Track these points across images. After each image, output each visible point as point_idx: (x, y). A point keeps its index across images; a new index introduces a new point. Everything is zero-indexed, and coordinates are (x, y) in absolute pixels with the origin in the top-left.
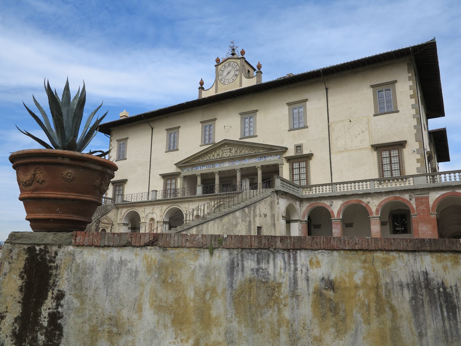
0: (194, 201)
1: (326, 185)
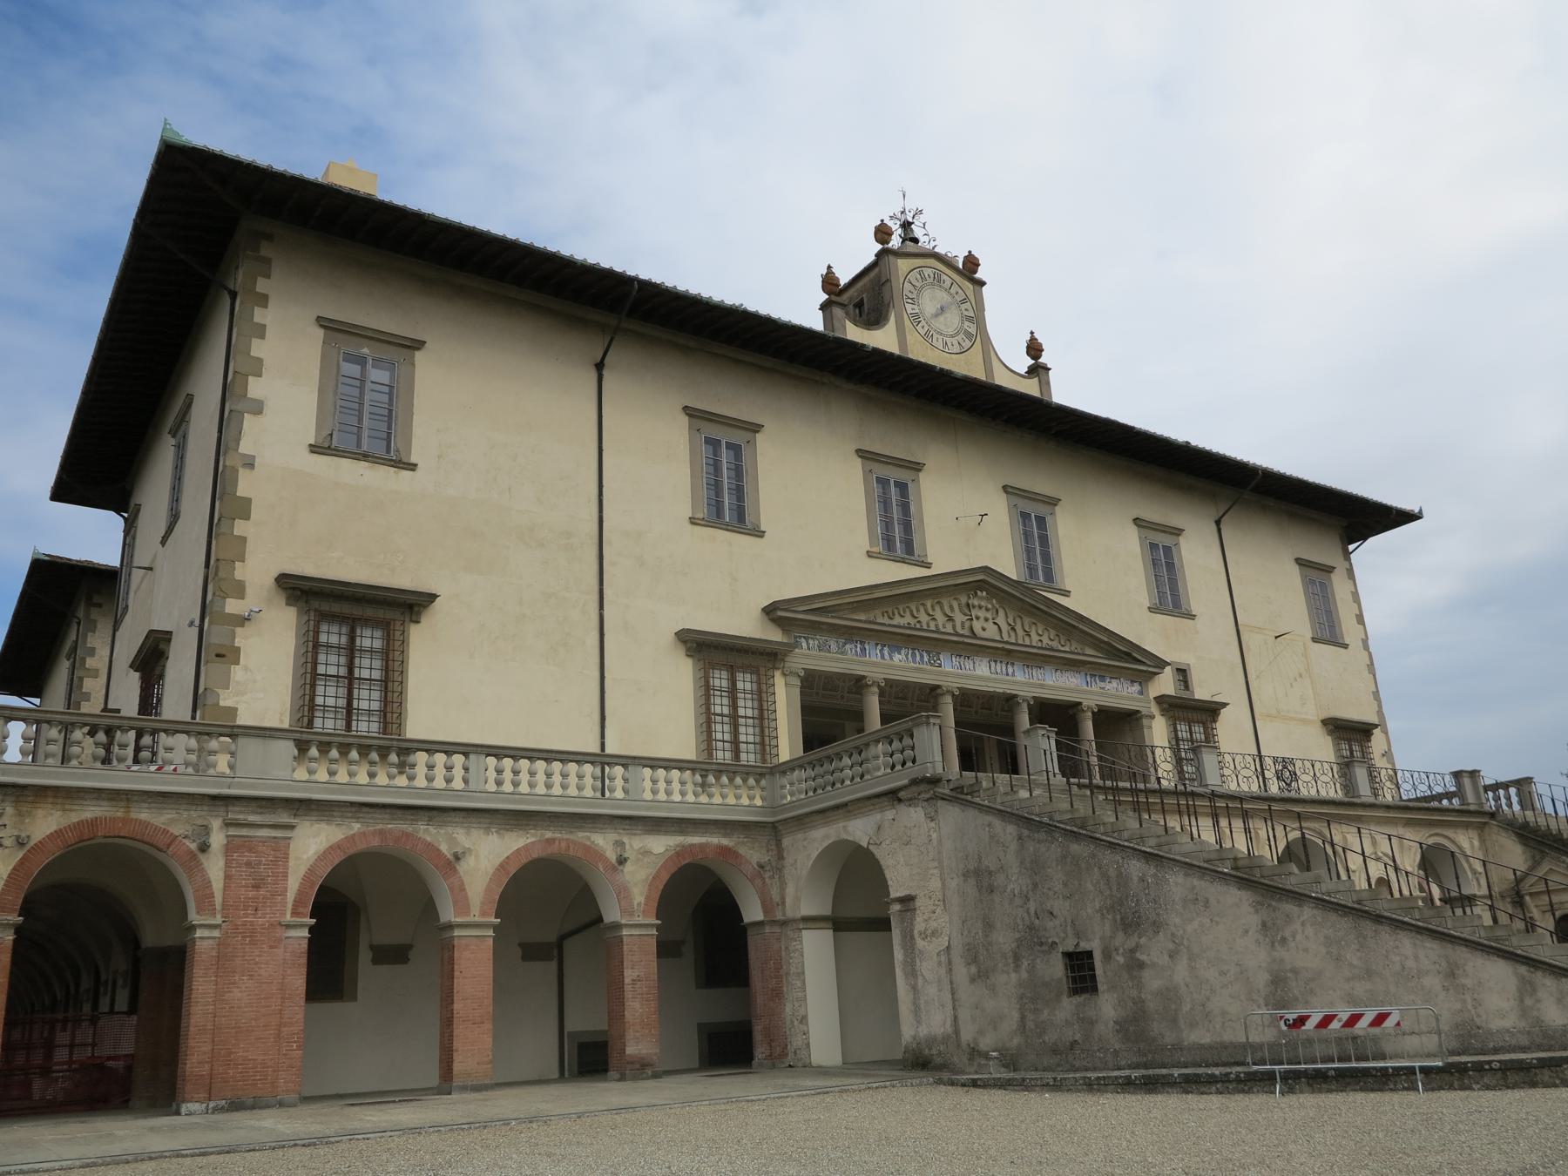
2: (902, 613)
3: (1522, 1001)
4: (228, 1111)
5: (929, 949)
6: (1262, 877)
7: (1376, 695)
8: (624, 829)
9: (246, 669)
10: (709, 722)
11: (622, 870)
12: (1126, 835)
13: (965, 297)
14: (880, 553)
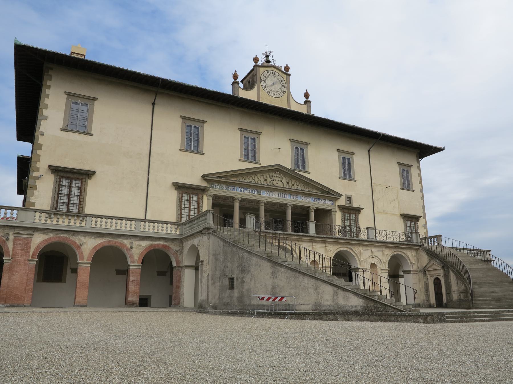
0: (369, 246)
1: (167, 223)
2: (249, 178)
3: (334, 297)
4: (10, 307)
5: (205, 275)
6: (274, 259)
7: (423, 207)
8: (133, 239)
9: (38, 191)
10: (181, 209)
11: (132, 250)
12: (244, 246)
13: (283, 79)
14: (243, 160)
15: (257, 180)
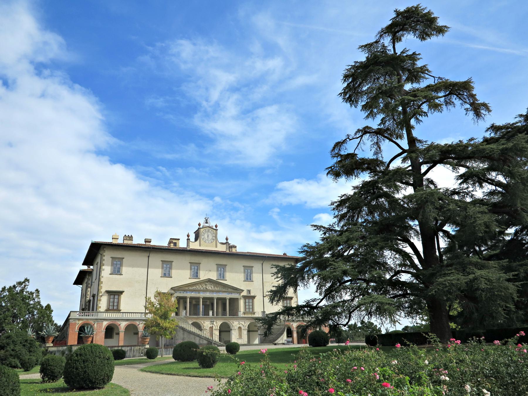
15: (198, 287)
